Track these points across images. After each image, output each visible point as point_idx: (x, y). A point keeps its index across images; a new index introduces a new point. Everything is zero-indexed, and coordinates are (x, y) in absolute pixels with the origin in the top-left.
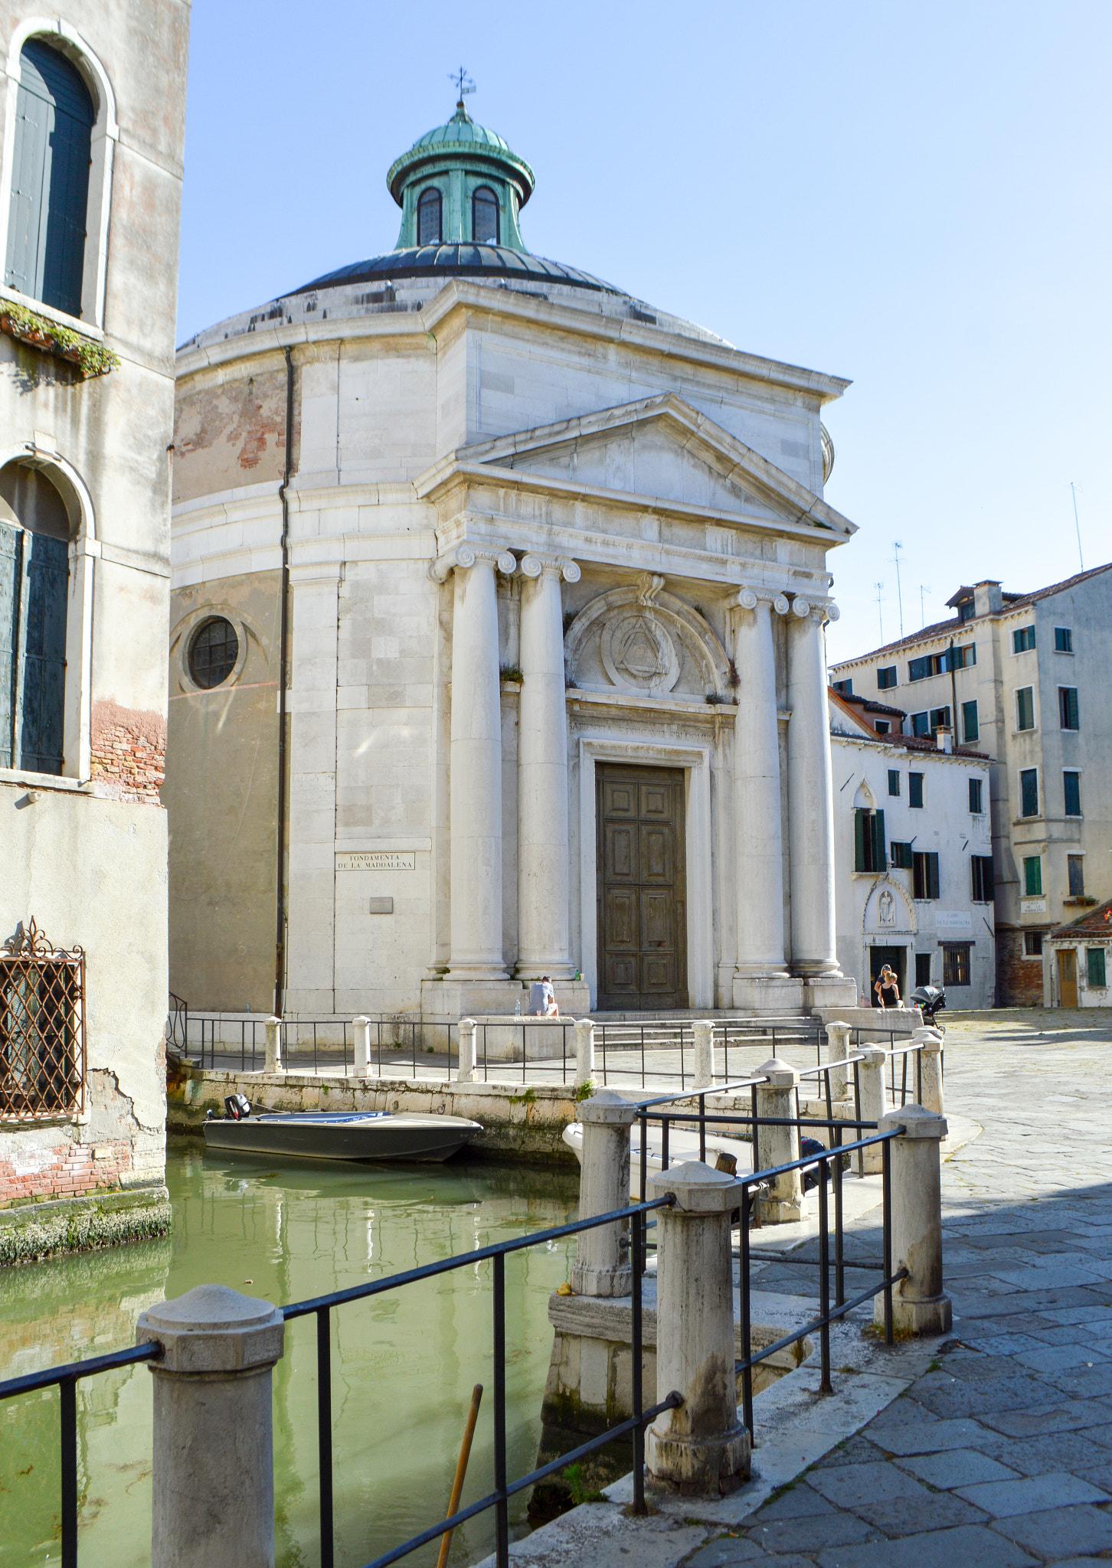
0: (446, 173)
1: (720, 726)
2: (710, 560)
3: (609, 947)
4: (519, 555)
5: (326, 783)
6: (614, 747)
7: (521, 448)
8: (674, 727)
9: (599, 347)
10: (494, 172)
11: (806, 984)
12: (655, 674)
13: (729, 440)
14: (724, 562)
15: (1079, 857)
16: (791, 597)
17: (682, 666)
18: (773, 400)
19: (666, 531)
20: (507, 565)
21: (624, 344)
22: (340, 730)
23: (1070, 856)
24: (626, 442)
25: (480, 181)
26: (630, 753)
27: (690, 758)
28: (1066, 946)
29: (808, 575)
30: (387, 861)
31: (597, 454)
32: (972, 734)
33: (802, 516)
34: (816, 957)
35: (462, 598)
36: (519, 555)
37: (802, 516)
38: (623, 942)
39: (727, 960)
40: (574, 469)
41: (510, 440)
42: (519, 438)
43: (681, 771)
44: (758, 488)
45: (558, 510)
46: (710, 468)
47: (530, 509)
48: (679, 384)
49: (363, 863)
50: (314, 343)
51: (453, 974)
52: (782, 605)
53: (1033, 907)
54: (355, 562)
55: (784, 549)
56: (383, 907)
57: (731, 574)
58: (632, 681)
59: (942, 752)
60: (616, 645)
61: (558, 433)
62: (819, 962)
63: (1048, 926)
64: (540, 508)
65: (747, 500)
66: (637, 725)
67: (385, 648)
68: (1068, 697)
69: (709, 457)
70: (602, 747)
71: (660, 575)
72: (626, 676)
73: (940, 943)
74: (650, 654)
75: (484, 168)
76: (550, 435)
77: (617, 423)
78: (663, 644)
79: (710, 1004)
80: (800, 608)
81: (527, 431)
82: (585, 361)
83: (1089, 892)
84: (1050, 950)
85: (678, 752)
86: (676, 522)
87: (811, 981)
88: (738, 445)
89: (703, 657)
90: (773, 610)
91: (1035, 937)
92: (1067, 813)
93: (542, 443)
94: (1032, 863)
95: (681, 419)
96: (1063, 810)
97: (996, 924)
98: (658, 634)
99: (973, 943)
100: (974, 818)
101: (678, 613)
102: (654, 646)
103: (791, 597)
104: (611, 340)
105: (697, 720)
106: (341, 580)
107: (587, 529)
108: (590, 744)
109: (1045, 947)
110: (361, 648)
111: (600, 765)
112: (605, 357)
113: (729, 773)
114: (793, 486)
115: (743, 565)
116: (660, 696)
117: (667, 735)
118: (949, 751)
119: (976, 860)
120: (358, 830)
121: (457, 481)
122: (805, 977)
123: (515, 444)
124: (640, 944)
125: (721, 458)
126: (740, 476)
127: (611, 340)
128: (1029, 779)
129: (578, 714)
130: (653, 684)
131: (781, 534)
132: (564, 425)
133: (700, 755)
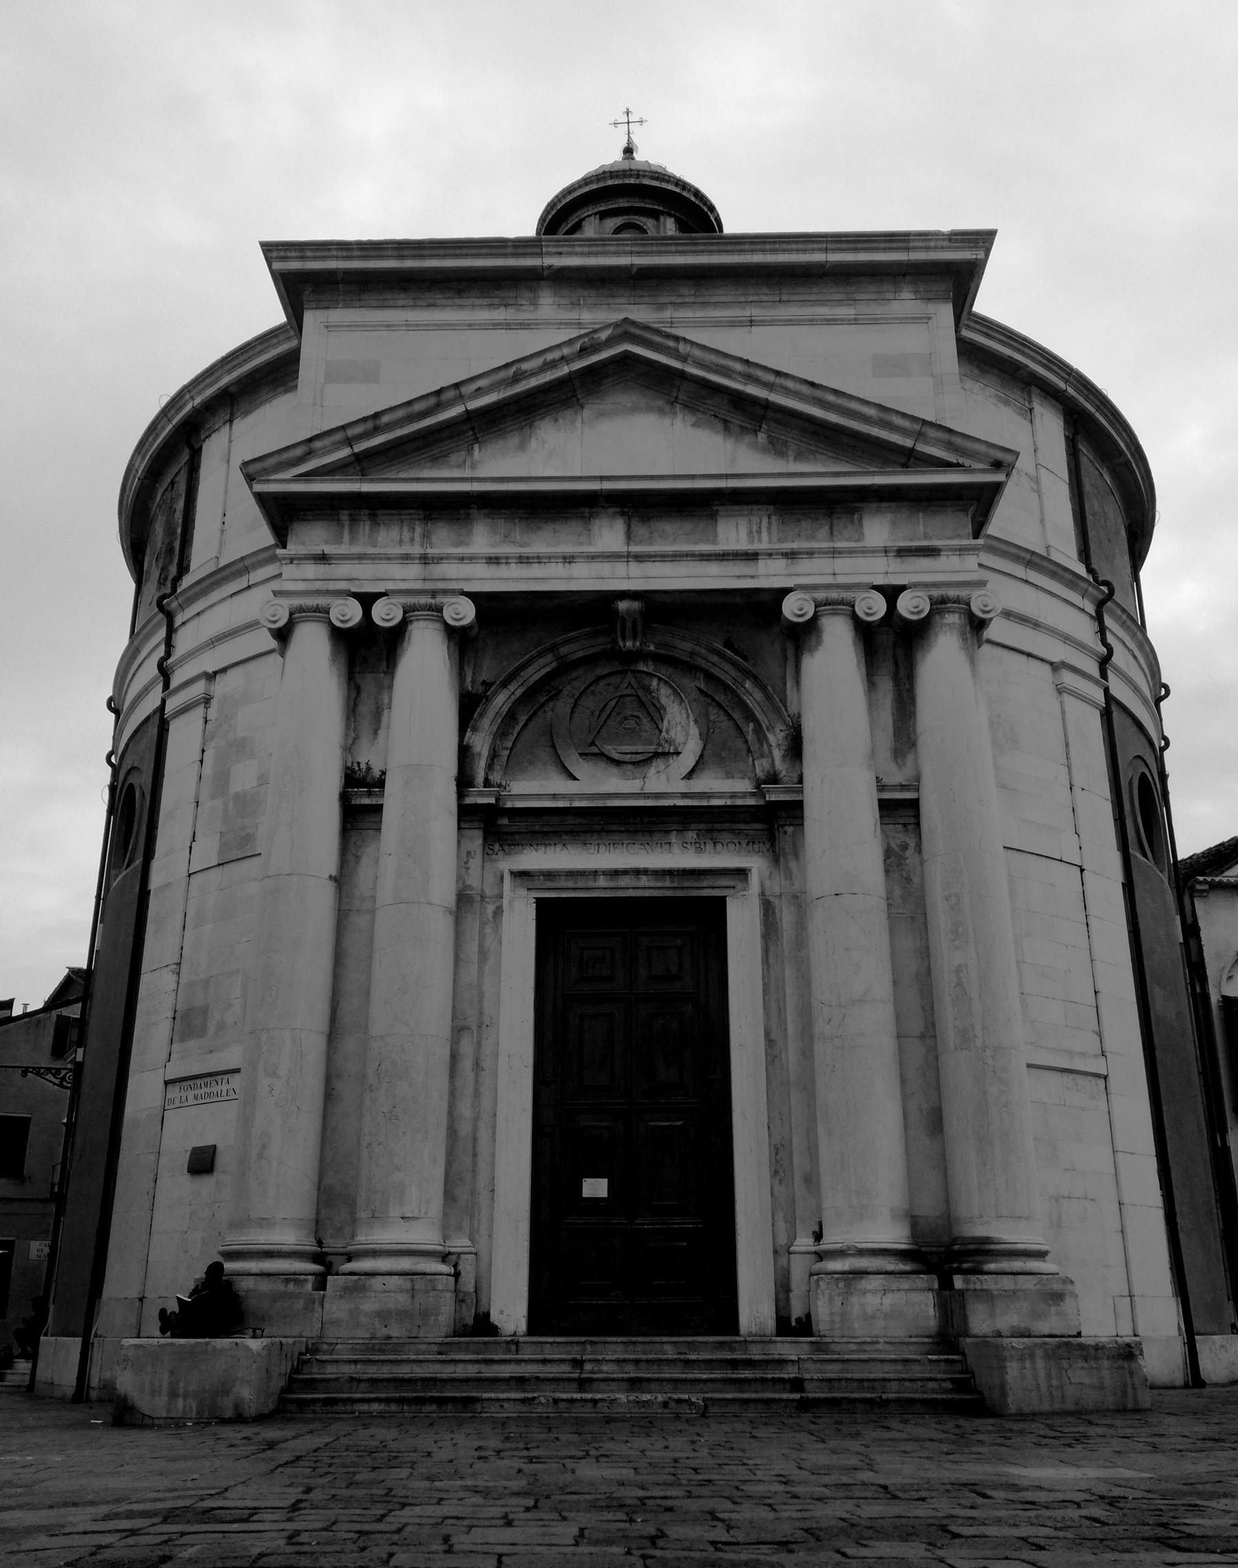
1: (773, 821)
2: (723, 557)
4: (367, 600)
5: (168, 979)
6: (571, 874)
7: (360, 447)
8: (691, 835)
13: (738, 367)
16: (891, 593)
17: (706, 737)
19: (640, 530)
20: (351, 613)
22: (191, 902)
24: (568, 414)
30: (215, 1089)
31: (514, 440)
33: (909, 458)
34: (979, 1231)
37: (909, 458)
40: (473, 467)
41: (338, 436)
42: (350, 433)
44: (815, 433)
46: (725, 422)
49: (191, 1094)
54: (224, 670)
57: (768, 575)
58: (614, 770)
65: (799, 457)
67: (243, 778)
70: (549, 875)
76: (412, 418)
77: (533, 382)
78: (669, 710)
79: (771, 1325)
80: (908, 606)
81: (365, 419)
87: (958, 1282)
88: (759, 373)
89: (750, 716)
93: (399, 432)
98: (664, 695)
102: (655, 713)
110: (222, 779)
111: (543, 906)
113: (799, 901)
114: (871, 412)
116: (665, 783)
120: (193, 1044)
123: (349, 442)
125: (740, 402)
129: (491, 824)
130: (653, 770)
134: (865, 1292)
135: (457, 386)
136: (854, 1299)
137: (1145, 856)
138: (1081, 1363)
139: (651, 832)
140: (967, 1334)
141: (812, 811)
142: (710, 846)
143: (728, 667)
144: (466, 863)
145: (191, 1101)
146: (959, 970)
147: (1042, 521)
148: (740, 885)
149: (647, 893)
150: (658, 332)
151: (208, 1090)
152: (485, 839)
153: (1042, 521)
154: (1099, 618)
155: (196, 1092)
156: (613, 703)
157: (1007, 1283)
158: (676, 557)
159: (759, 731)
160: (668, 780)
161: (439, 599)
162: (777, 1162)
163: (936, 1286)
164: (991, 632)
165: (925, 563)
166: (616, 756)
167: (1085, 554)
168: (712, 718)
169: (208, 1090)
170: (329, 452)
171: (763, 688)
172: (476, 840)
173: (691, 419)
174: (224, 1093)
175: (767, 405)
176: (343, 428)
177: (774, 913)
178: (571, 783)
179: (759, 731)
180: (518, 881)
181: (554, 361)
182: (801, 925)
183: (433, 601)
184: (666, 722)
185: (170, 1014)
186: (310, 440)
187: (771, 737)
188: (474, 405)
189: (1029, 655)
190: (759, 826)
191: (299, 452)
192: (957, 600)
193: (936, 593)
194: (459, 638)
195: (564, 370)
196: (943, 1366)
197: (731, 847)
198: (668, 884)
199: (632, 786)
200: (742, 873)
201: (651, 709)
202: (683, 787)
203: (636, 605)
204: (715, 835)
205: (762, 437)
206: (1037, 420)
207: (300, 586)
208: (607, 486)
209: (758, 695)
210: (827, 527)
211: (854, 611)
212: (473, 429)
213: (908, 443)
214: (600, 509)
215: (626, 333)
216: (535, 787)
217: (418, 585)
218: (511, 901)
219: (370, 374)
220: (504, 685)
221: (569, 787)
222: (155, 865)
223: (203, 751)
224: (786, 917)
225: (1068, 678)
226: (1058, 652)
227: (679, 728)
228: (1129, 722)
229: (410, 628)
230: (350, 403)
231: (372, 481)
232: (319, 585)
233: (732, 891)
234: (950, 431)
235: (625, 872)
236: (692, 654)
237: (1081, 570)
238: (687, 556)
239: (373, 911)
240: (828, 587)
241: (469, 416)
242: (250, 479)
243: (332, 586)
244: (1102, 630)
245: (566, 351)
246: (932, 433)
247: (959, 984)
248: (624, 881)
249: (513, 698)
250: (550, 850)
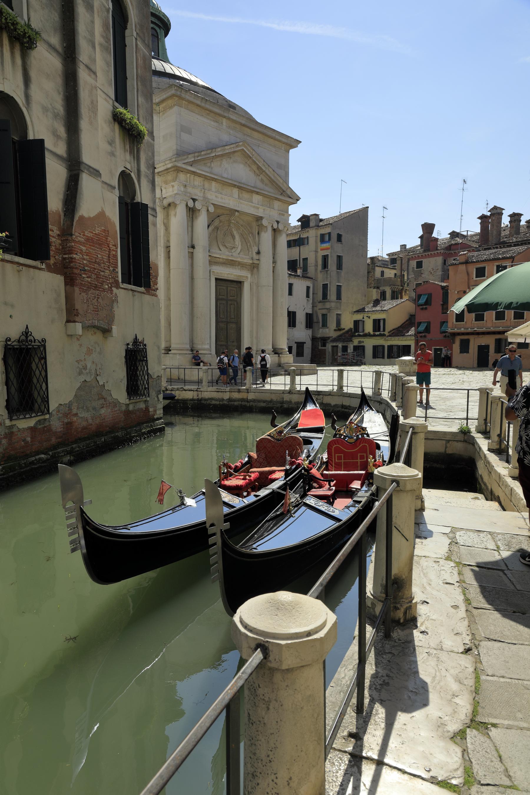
2: (254, 207)
6: (221, 273)
7: (196, 159)
11: (279, 356)
14: (258, 208)
15: (340, 315)
20: (191, 204)
21: (229, 119)
23: (337, 314)
26: (226, 275)
28: (334, 344)
32: (305, 269)
34: (281, 347)
35: (175, 215)
36: (194, 200)
41: (193, 155)
43: (240, 282)
45: (207, 185)
47: (197, 183)
51: (172, 352)
52: (275, 226)
53: (324, 331)
55: (277, 204)
59: (299, 276)
61: (208, 154)
62: (282, 349)
63: (329, 338)
65: (266, 185)
66: (229, 266)
68: (339, 258)
69: (254, 167)
70: (217, 273)
73: (296, 343)
74: (232, 240)
76: (205, 155)
80: (281, 227)
82: (216, 124)
83: (342, 326)
84: (329, 346)
85: (240, 276)
86: (244, 192)
87: (280, 355)
90: (272, 226)
91: (324, 340)
92: (337, 299)
93: (203, 157)
94: (324, 316)
95: (248, 152)
96: (336, 299)
97: (312, 336)
99: (305, 343)
100: (308, 300)
101: (242, 226)
102: (233, 237)
103: (278, 222)
104: (225, 117)
105: (246, 265)
107: (216, 192)
109: (327, 345)
111: (216, 279)
112: (222, 123)
115: (264, 210)
118: (301, 276)
119: (307, 314)
121: (173, 169)
122: (279, 354)
123: (194, 157)
124: (227, 342)
125: (259, 168)
126: (264, 175)
127: (225, 117)
128: (325, 287)
130: (233, 251)
133: (247, 277)
157: (285, 355)
208: (240, 185)
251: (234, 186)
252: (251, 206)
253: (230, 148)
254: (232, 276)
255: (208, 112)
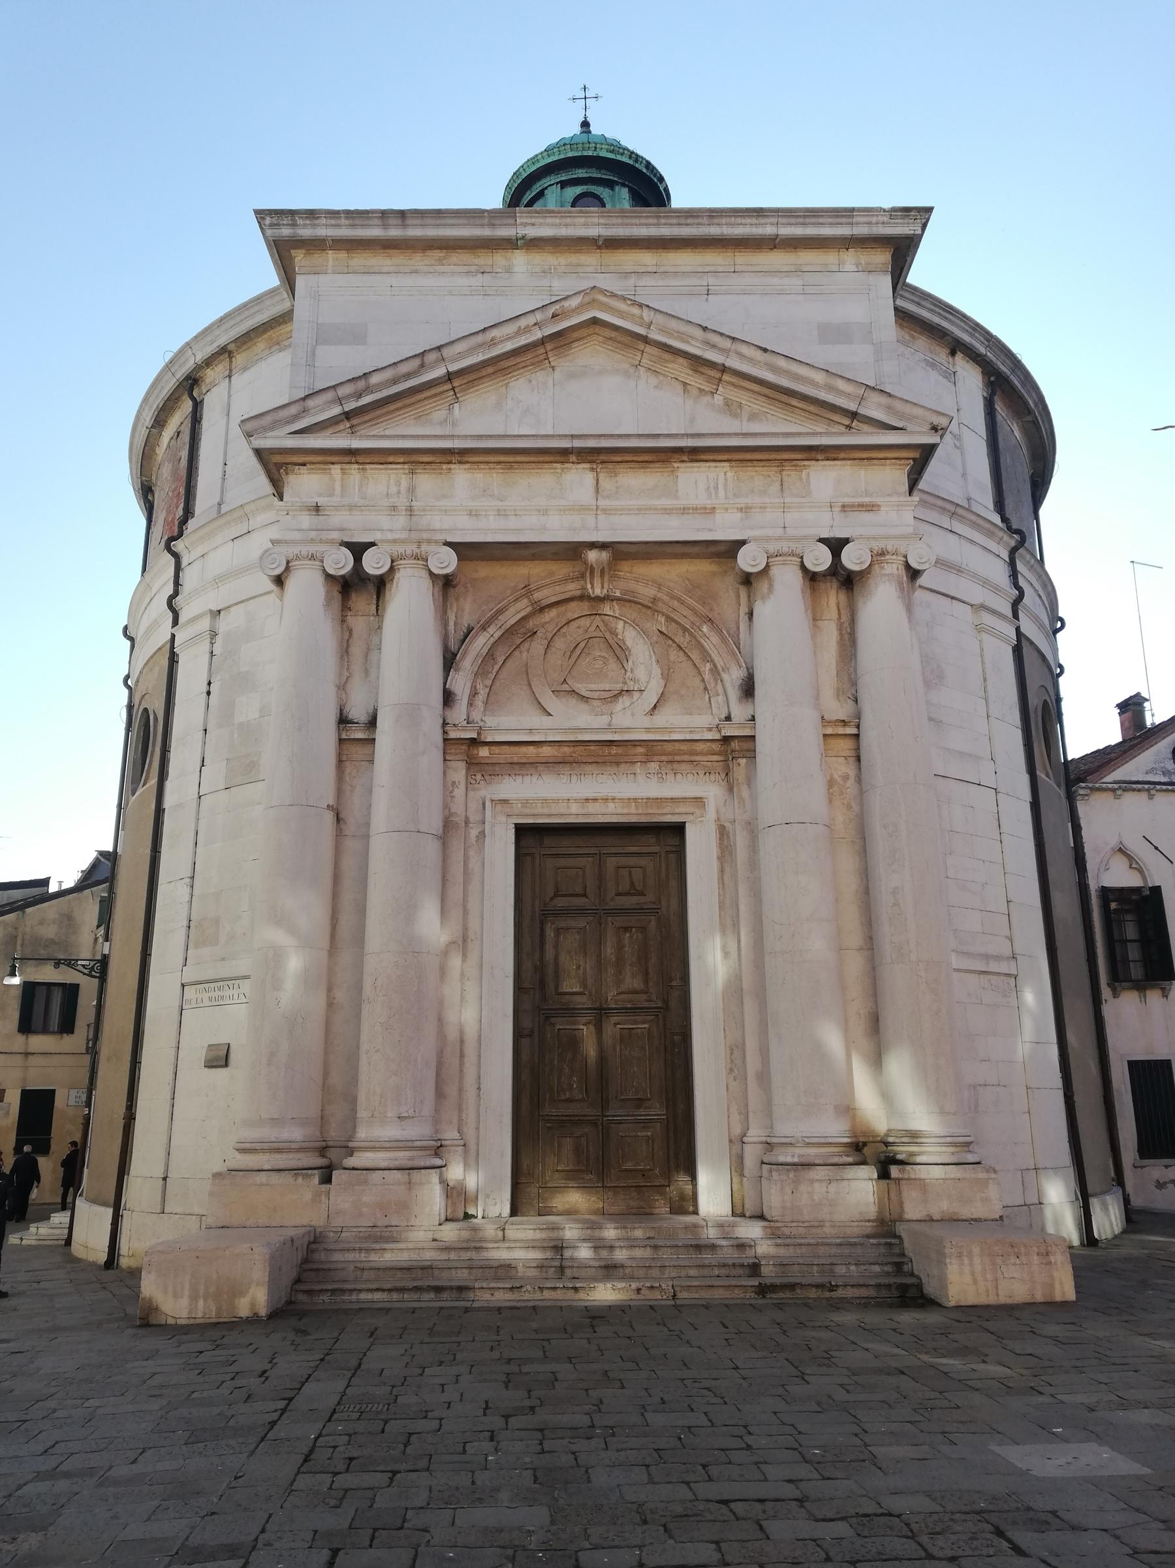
0: (541, 194)
3: (549, 1110)
4: (358, 550)
7: (351, 405)
8: (654, 766)
9: (499, 259)
10: (595, 174)
11: (884, 1175)
12: (621, 693)
16: (836, 546)
17: (667, 677)
18: (799, 271)
19: (606, 483)
20: (341, 563)
24: (540, 376)
25: (579, 190)
26: (574, 808)
27: (682, 809)
29: (871, 508)
38: (569, 1101)
39: (755, 1133)
40: (454, 425)
41: (330, 395)
42: (342, 392)
45: (426, 482)
46: (685, 384)
48: (632, 281)
49: (206, 996)
50: (209, 362)
56: (220, 1059)
58: (584, 706)
60: (556, 658)
61: (408, 376)
64: (398, 484)
65: (753, 417)
66: (588, 768)
67: (248, 709)
69: (679, 368)
70: (526, 802)
71: (603, 546)
72: (573, 701)
74: (613, 664)
75: (581, 173)
76: (395, 381)
82: (478, 281)
85: (660, 801)
87: (894, 1171)
89: (707, 657)
90: (803, 567)
98: (630, 636)
102: (620, 653)
106: (213, 634)
108: (504, 801)
111: (523, 832)
116: (630, 720)
117: (641, 778)
123: (340, 401)
125: (698, 363)
131: (813, 452)
132: (416, 363)
134: (812, 1181)
135: (439, 348)
136: (803, 1188)
137: (1048, 776)
138: (1013, 1259)
139: (618, 764)
140: (901, 1220)
141: (763, 745)
142: (671, 777)
143: (686, 612)
144: (452, 792)
145: (206, 1002)
146: (895, 891)
147: (964, 475)
148: (698, 812)
149: (614, 819)
150: (624, 298)
151: (221, 993)
152: (468, 769)
153: (964, 475)
154: (1012, 564)
155: (210, 995)
156: (582, 645)
158: (641, 510)
159: (715, 671)
160: (633, 715)
161: (425, 548)
162: (732, 1061)
163: (876, 1176)
164: (922, 580)
165: (866, 517)
166: (585, 694)
167: (1000, 506)
168: (672, 658)
169: (221, 993)
170: (323, 411)
171: (719, 632)
172: (459, 772)
173: (653, 380)
174: (236, 997)
175: (724, 369)
176: (334, 387)
177: (728, 837)
178: (546, 718)
179: (715, 671)
180: (499, 807)
181: (527, 327)
182: (753, 848)
183: (418, 551)
184: (630, 662)
185: (185, 923)
186: (304, 399)
187: (725, 676)
188: (454, 367)
189: (953, 598)
190: (716, 758)
191: (293, 410)
192: (896, 553)
193: (877, 546)
194: (446, 584)
195: (538, 335)
196: (882, 1250)
197: (690, 776)
198: (633, 811)
199: (602, 721)
200: (699, 801)
201: (618, 651)
202: (646, 722)
203: (605, 555)
204: (675, 766)
205: (718, 399)
206: (960, 383)
207: (297, 536)
208: (578, 444)
209: (715, 639)
210: (778, 484)
211: (802, 562)
212: (453, 389)
213: (852, 407)
214: (574, 466)
215: (594, 300)
216: (512, 721)
217: (404, 535)
218: (493, 825)
219: (355, 336)
220: (484, 628)
221: (546, 721)
222: (169, 785)
223: (209, 684)
224: (741, 841)
225: (988, 619)
226: (977, 595)
227: (642, 667)
228: (1035, 654)
229: (397, 576)
230: (341, 362)
231: (361, 437)
232: (313, 534)
233: (691, 818)
234: (890, 395)
235: (595, 800)
236: (655, 600)
237: (997, 519)
238: (650, 509)
239: (367, 837)
240: (779, 539)
241: (450, 377)
242: (249, 435)
243: (325, 535)
244: (1014, 575)
245: (539, 316)
246: (875, 398)
247: (896, 904)
248: (592, 808)
249: (492, 640)
250: (527, 779)
251: (563, 455)
252: (667, 511)
253: (519, 333)
254: (611, 807)
255: (438, 254)
